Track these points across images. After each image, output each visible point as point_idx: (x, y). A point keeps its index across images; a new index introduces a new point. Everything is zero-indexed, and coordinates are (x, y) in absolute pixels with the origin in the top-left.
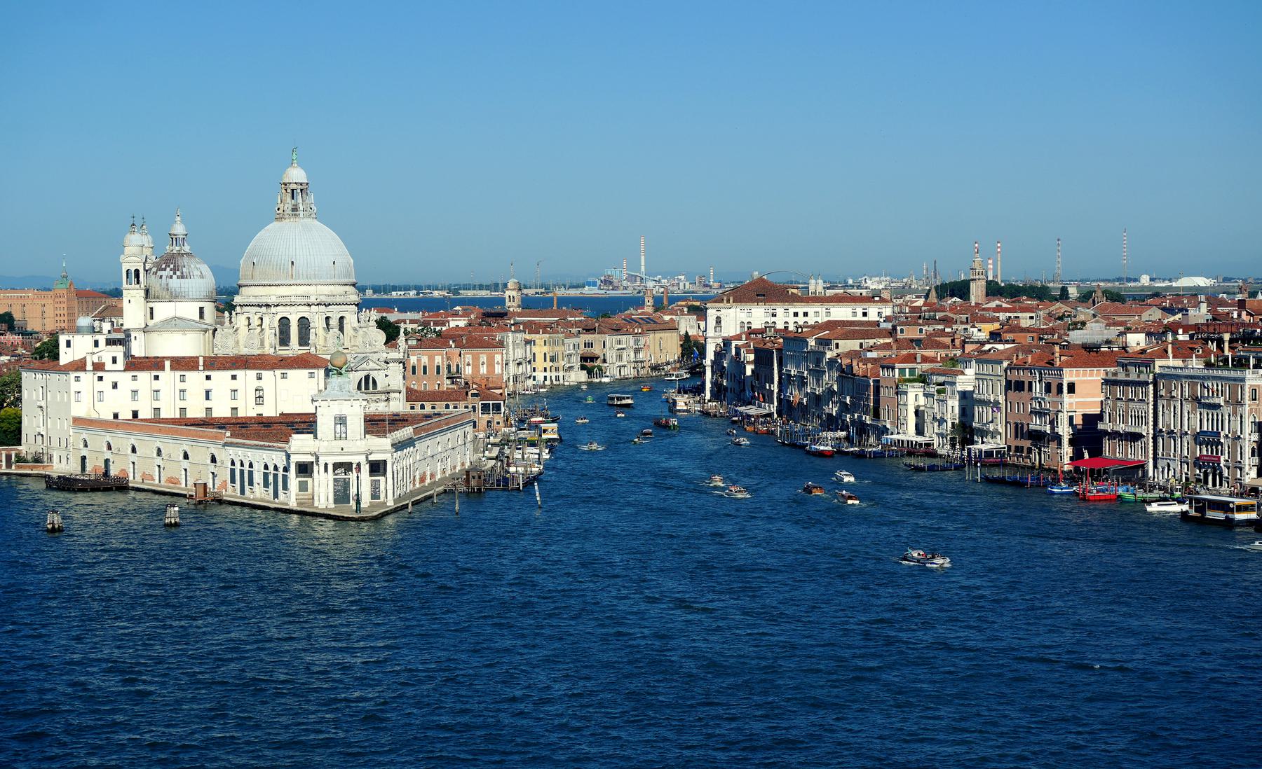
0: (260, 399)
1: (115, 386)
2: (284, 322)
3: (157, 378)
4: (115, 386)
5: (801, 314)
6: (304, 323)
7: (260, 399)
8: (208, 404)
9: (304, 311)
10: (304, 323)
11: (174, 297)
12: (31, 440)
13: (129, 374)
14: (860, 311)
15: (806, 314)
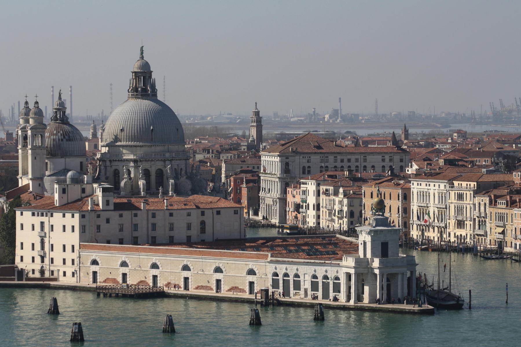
0: (203, 230)
1: (108, 221)
2: (147, 174)
3: (136, 215)
4: (108, 221)
5: (346, 160)
6: (160, 174)
7: (203, 230)
8: (152, 234)
9: (159, 165)
10: (160, 174)
11: (64, 155)
12: (28, 259)
13: (117, 213)
14: (387, 158)
15: (349, 160)
